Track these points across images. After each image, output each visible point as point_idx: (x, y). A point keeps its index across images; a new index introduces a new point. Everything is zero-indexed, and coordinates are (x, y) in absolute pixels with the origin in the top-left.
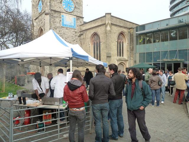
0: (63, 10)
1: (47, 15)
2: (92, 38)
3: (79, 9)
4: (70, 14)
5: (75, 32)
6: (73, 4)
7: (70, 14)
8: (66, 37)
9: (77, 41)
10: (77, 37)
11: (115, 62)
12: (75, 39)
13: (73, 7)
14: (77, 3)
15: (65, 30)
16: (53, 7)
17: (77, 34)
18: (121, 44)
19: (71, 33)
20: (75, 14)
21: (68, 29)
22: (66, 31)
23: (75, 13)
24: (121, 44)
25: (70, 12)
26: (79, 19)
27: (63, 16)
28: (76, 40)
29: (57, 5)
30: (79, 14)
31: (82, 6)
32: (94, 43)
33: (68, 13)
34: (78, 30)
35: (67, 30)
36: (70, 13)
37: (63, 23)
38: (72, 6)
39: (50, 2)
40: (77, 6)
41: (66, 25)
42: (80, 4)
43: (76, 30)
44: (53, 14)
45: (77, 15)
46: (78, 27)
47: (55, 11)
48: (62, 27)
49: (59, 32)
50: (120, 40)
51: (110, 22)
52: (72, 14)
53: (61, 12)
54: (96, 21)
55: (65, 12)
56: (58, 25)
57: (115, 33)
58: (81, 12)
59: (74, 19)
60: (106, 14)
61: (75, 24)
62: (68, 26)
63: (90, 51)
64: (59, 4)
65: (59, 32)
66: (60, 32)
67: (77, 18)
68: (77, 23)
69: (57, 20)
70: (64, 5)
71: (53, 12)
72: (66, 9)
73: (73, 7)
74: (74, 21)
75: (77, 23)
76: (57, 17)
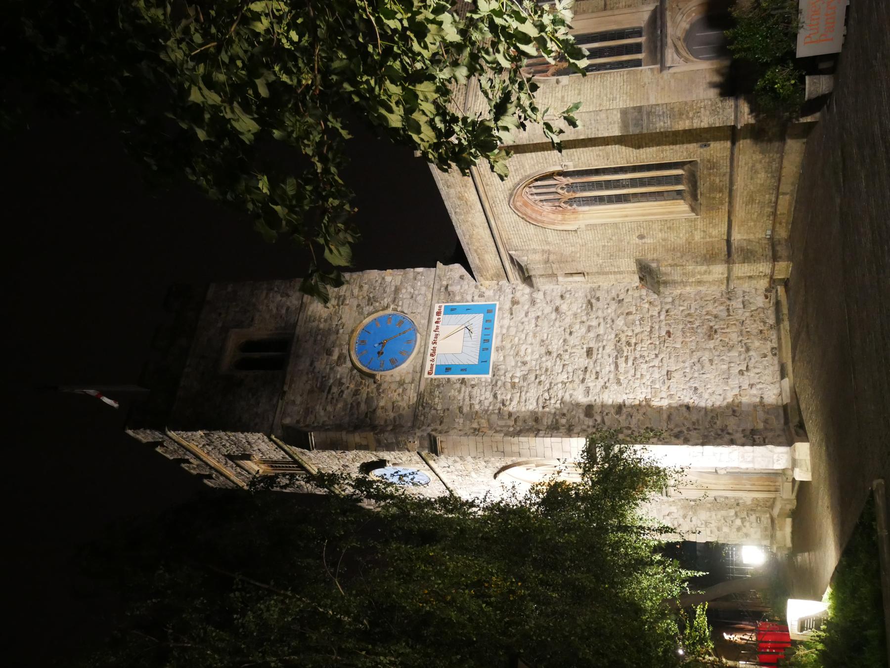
14: (369, 299)
32: (570, 202)
63: (615, 225)
68: (469, 298)
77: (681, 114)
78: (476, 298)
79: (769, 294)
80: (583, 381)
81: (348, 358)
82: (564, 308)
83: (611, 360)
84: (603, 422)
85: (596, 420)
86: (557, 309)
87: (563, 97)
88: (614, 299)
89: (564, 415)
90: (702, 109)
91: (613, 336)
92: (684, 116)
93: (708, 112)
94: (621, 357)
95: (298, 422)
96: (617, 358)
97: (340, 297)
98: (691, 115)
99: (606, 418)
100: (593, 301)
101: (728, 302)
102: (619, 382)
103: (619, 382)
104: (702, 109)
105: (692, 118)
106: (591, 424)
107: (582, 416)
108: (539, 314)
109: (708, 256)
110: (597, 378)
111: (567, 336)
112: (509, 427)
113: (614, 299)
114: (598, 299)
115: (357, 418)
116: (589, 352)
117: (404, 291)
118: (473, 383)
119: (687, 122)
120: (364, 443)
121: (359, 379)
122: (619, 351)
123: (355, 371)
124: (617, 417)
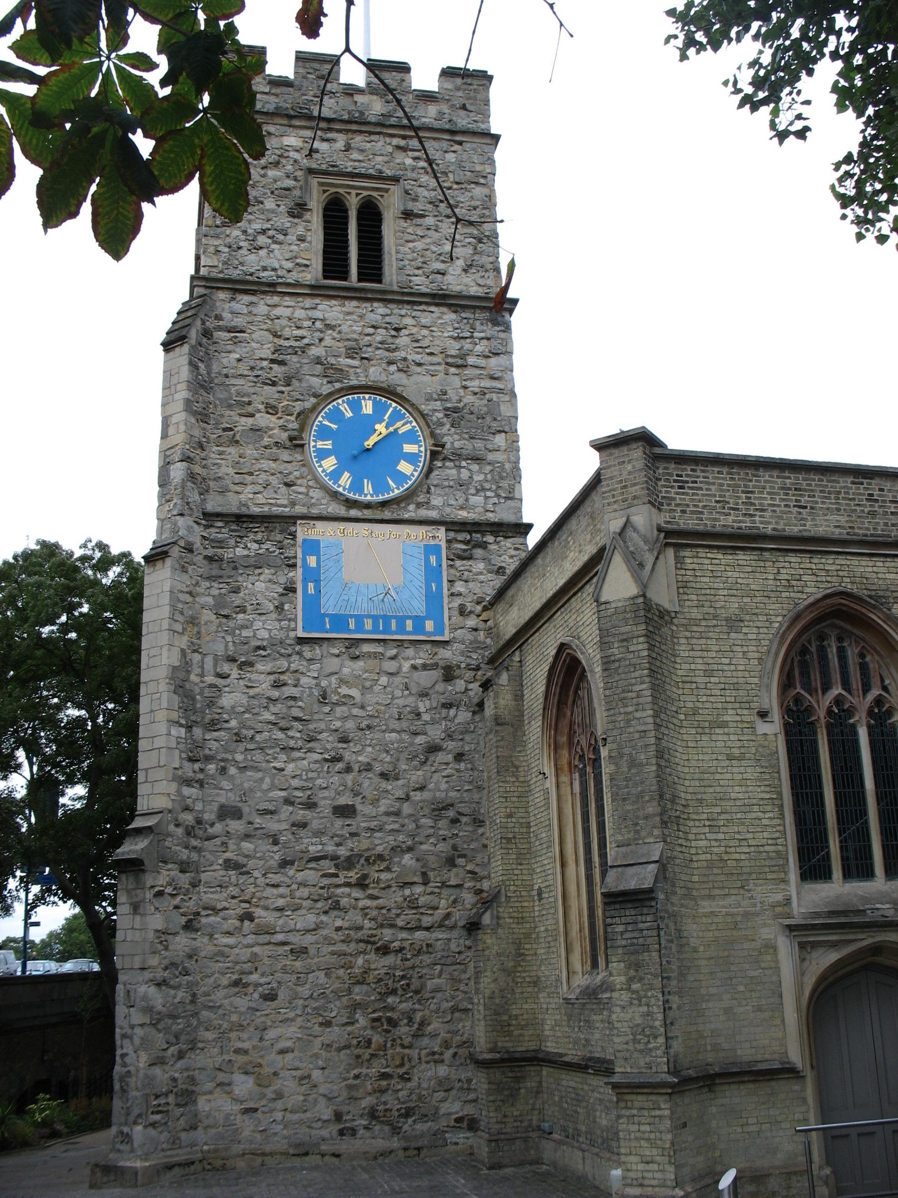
0: (316, 494)
1: (159, 564)
2: (561, 704)
3: (477, 459)
4: (387, 514)
5: (436, 674)
6: (412, 431)
7: (387, 514)
8: (350, 725)
9: (459, 757)
10: (463, 716)
11: (771, 947)
12: (436, 733)
13: (412, 458)
14: (456, 410)
15: (333, 664)
16: (223, 491)
17: (460, 685)
18: (863, 734)
19: (397, 680)
20: (433, 514)
21: (366, 648)
22: (350, 668)
23: (440, 503)
24: (863, 734)
25: (384, 504)
26: (484, 546)
27: (313, 547)
28: (451, 745)
29: (265, 464)
30: (477, 500)
31: (509, 428)
33: (368, 513)
34: (476, 646)
35: (360, 663)
36: (385, 512)
37: (312, 603)
38: (409, 448)
39: (186, 459)
40: (453, 440)
41: (339, 621)
42: (492, 411)
43: (445, 654)
44: (220, 544)
45: (463, 514)
46: (471, 622)
47: (241, 520)
48: (301, 641)
49: (277, 685)
50: (837, 690)
51: (643, 518)
52: (411, 512)
53: (293, 519)
54: (563, 535)
55: (342, 511)
56: (264, 629)
57: (733, 624)
58: (504, 484)
59: (430, 550)
60: (602, 446)
61: (433, 600)
62: (360, 628)
64: (285, 455)
65: (277, 685)
66: (288, 691)
67: (461, 536)
68: (459, 587)
69: (261, 587)
70: (323, 454)
71: (220, 532)
72: (346, 479)
73: (412, 458)
74: (432, 574)
75: (459, 587)
76: (257, 564)
77: (637, 966)
78: (458, 601)
79: (465, 1125)
80: (288, 802)
81: (338, 385)
82: (441, 757)
83: (330, 848)
84: (208, 839)
85: (212, 825)
86: (433, 749)
87: (724, 725)
88: (455, 848)
89: (223, 770)
90: (645, 1009)
91: (380, 849)
92: (632, 973)
93: (638, 1020)
94: (337, 866)
95: (218, 318)
96: (334, 858)
97: (463, 357)
98: (636, 986)
99: (218, 841)
100: (451, 813)
101: (448, 1054)
102: (285, 863)
103: (285, 863)
104: (645, 1009)
105: (629, 989)
106: (206, 816)
107: (222, 800)
108: (426, 717)
109: (505, 1018)
110: (293, 825)
111: (378, 768)
112: (202, 675)
113: (455, 848)
114: (454, 821)
115: (222, 416)
116: (345, 812)
117: (475, 467)
118: (286, 607)
119: (623, 979)
120: (171, 431)
121: (298, 409)
122: (349, 863)
123: (313, 400)
124: (221, 861)
